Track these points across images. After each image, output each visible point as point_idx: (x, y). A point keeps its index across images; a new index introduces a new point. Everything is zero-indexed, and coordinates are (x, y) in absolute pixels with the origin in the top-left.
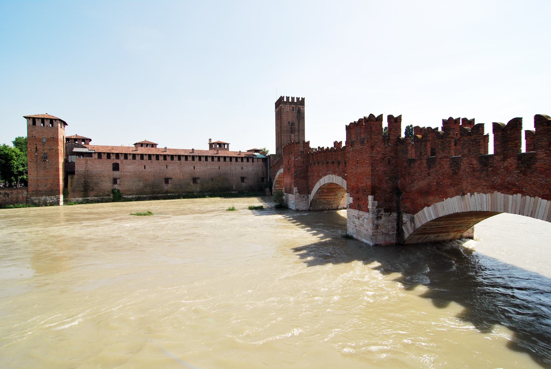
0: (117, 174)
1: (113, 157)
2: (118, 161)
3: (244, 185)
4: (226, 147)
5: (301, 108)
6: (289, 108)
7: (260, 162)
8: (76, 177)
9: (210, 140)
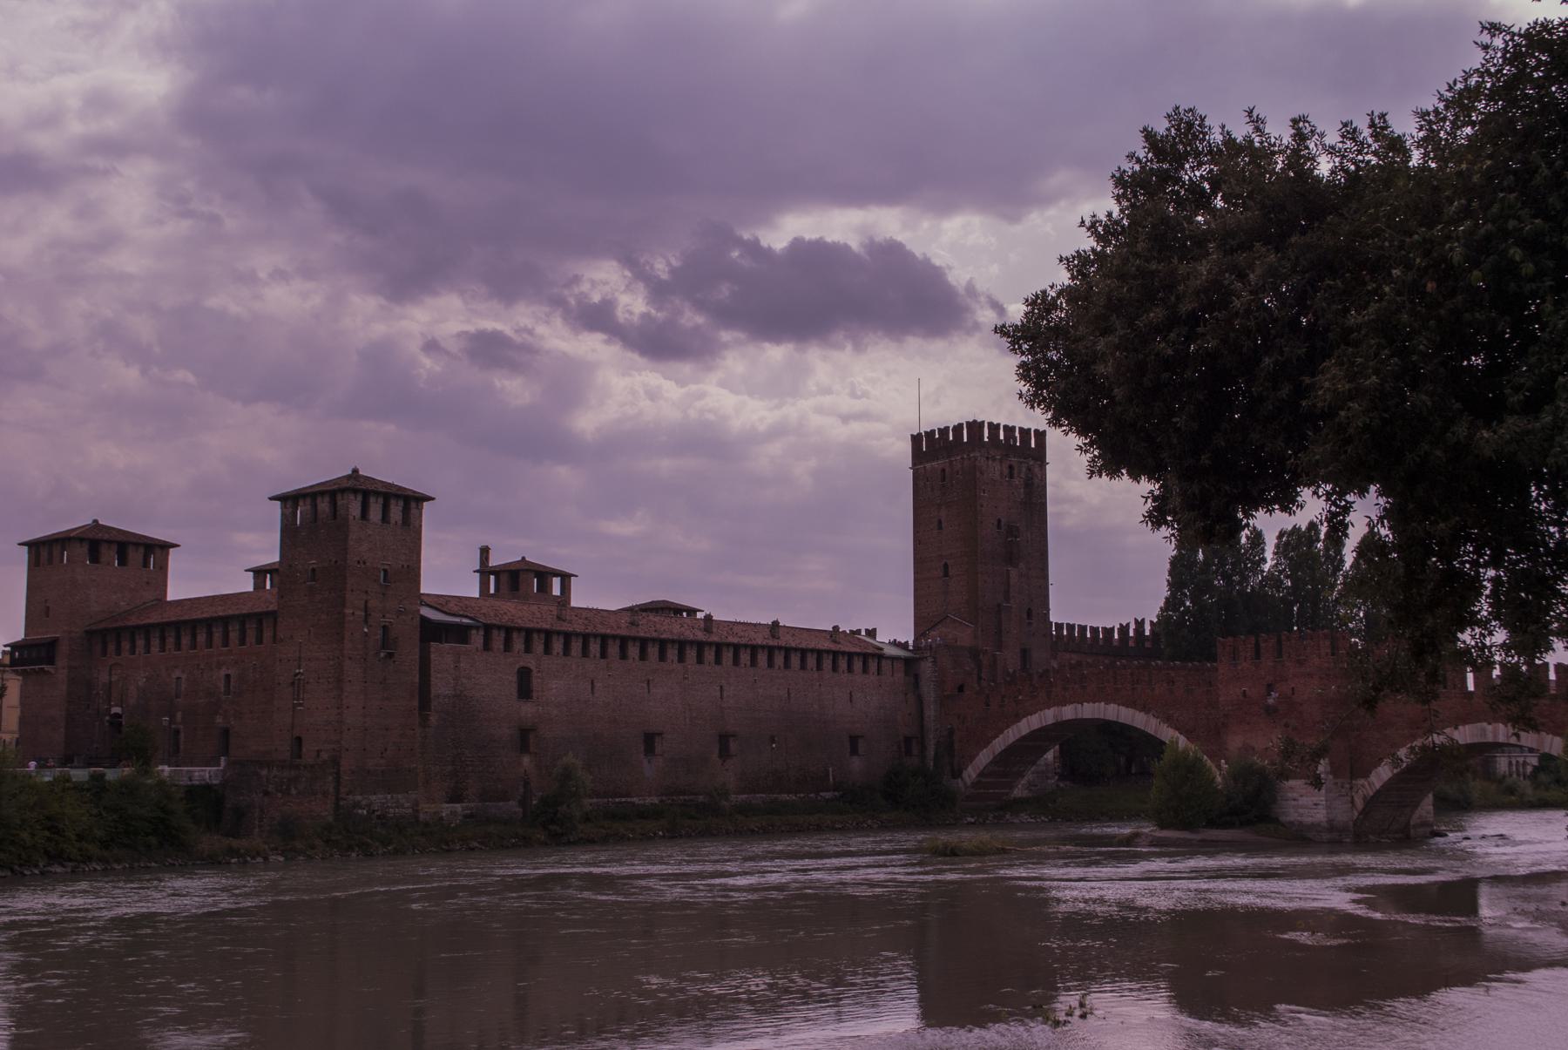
0: (527, 710)
1: (518, 643)
2: (530, 661)
3: (856, 764)
4: (556, 591)
5: (1036, 469)
6: (998, 467)
7: (900, 675)
8: (433, 719)
9: (485, 552)
